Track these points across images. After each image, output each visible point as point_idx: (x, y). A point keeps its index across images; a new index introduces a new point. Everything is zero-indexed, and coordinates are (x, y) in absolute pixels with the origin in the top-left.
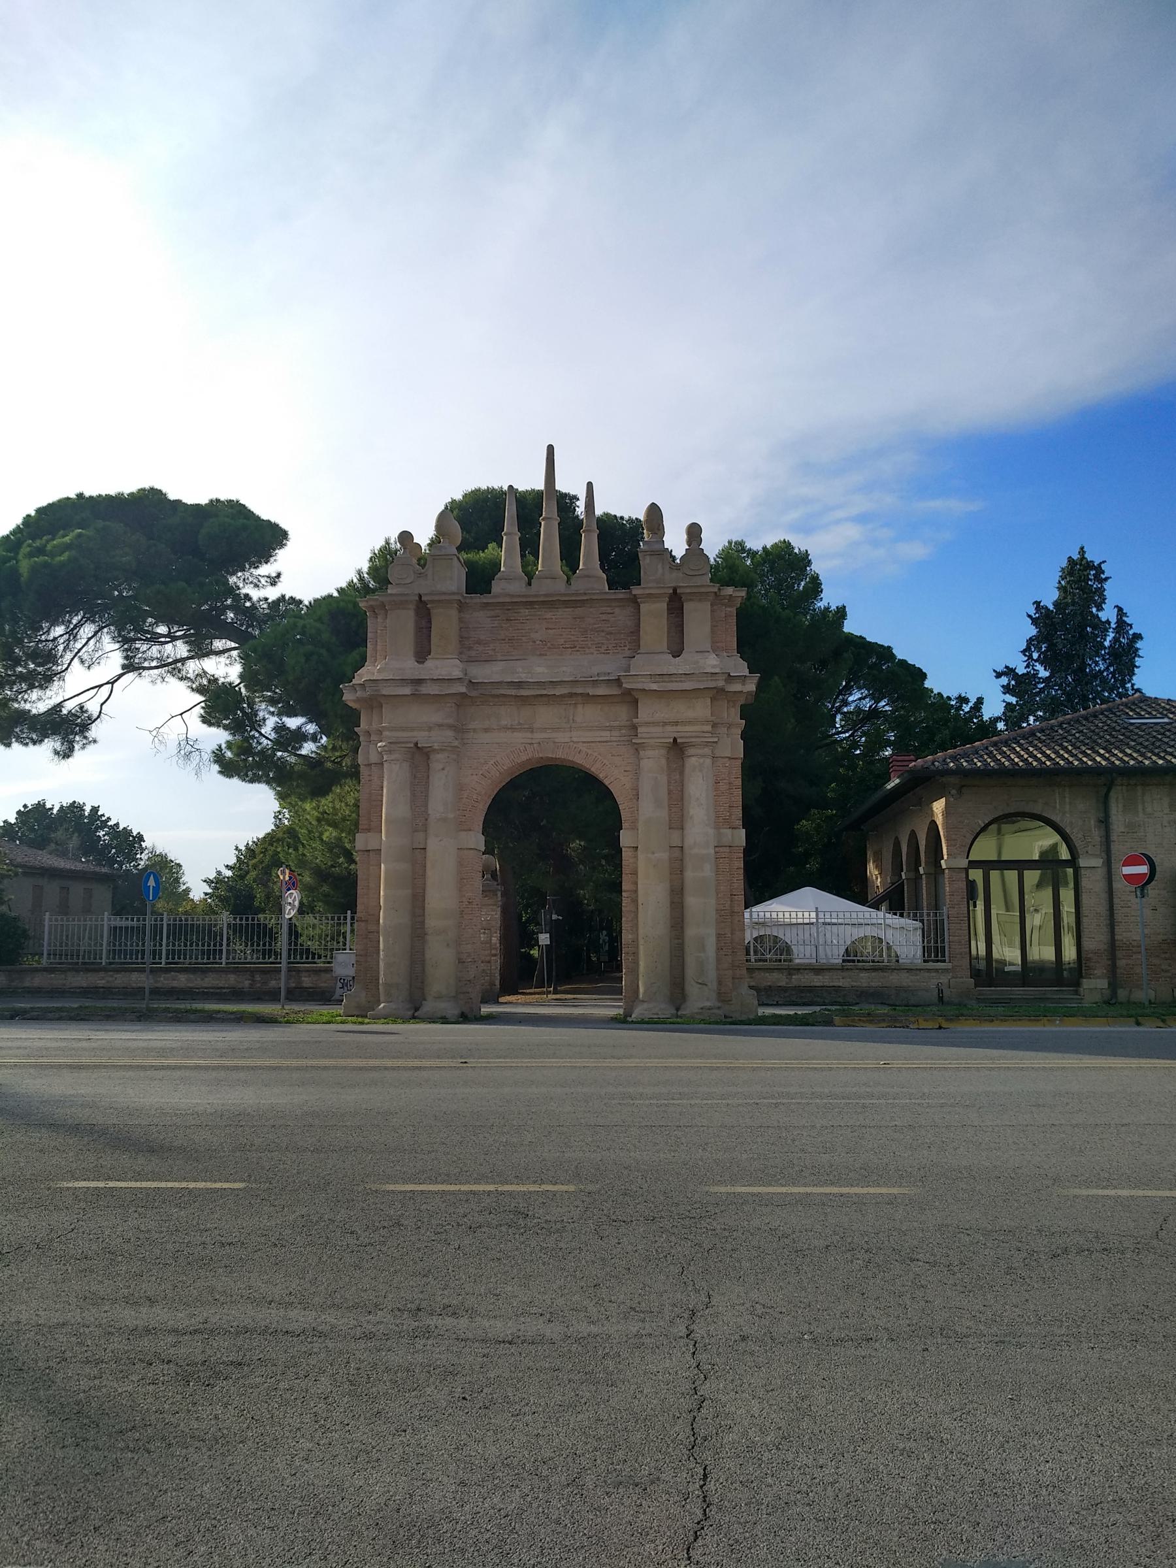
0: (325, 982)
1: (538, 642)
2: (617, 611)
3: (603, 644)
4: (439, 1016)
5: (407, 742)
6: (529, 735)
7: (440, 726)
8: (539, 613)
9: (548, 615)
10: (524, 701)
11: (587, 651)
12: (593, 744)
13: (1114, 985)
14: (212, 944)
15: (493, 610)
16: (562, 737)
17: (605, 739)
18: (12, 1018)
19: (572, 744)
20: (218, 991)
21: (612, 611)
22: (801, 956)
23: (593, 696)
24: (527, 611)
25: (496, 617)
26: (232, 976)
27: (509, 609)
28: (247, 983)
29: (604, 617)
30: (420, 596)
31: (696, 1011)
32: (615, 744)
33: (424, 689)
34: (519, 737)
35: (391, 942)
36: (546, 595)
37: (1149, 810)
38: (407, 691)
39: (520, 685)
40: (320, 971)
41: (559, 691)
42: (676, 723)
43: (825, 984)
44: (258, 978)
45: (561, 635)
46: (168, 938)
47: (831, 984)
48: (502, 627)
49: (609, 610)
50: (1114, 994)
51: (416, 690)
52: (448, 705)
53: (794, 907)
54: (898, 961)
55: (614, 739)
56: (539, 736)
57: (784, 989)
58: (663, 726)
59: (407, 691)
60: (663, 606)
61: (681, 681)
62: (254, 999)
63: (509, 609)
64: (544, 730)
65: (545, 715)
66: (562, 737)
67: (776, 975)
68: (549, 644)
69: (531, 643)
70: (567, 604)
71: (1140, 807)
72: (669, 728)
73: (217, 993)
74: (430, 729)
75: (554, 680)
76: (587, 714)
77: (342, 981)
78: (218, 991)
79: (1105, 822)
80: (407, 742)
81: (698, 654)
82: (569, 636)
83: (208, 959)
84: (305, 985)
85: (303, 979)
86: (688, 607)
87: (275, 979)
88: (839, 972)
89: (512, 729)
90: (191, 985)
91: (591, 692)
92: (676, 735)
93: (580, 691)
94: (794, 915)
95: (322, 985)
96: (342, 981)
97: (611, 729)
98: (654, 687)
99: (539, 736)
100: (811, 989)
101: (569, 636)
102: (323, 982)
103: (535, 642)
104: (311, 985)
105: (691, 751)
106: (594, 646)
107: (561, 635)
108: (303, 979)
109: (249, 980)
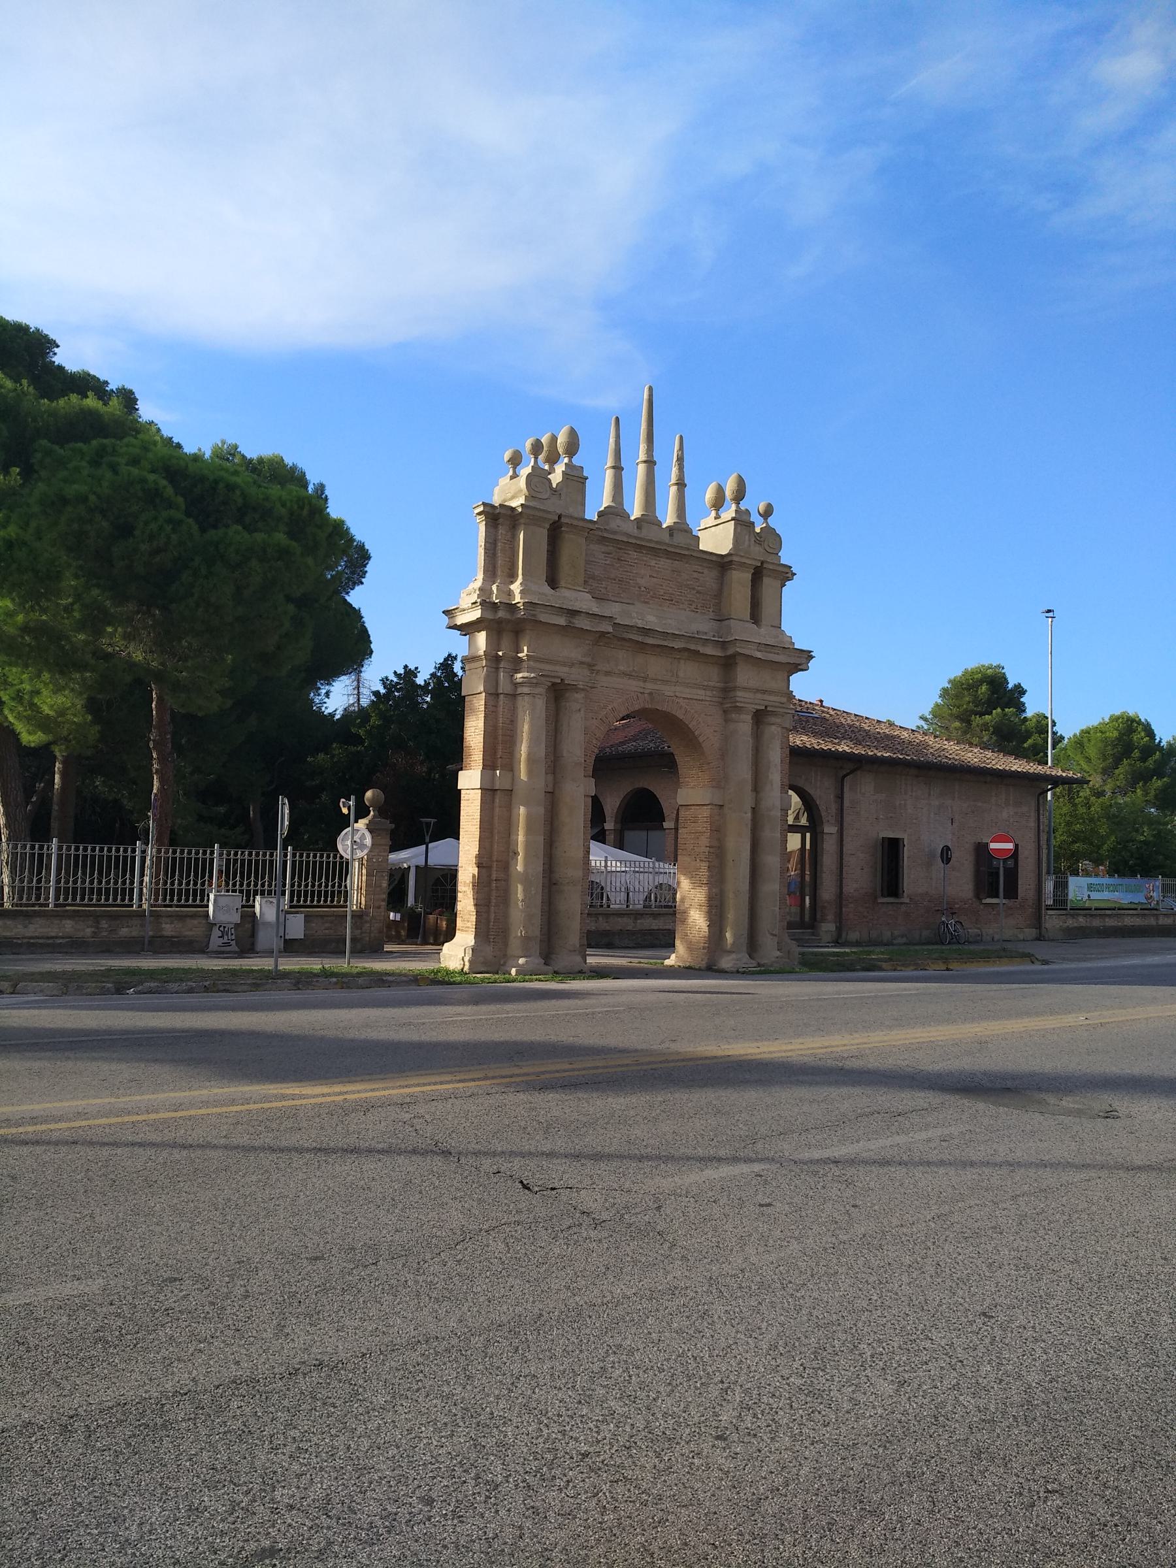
0: (191, 930)
1: (643, 589)
2: (706, 571)
3: (693, 601)
4: (577, 970)
5: (554, 677)
6: (642, 684)
7: (582, 663)
8: (645, 558)
9: (653, 563)
10: (642, 647)
11: (681, 606)
12: (691, 701)
13: (839, 930)
14: (88, 880)
15: (607, 546)
16: (668, 690)
17: (698, 697)
18: (120, 990)
19: (675, 698)
20: (50, 941)
21: (701, 571)
22: (618, 902)
23: (703, 654)
24: (635, 554)
25: (609, 554)
26: (68, 922)
27: (620, 549)
28: (89, 931)
29: (696, 575)
30: (560, 517)
31: (774, 959)
32: (707, 703)
33: (576, 622)
34: (634, 685)
35: (533, 892)
36: (657, 542)
37: (863, 791)
38: (561, 621)
39: (646, 631)
40: (186, 916)
41: (677, 645)
42: (764, 692)
43: (661, 927)
44: (104, 924)
45: (662, 585)
46: (293, 878)
47: (665, 927)
48: (613, 565)
49: (700, 569)
50: (839, 934)
51: (570, 622)
52: (587, 642)
53: (598, 856)
54: (609, 906)
55: (708, 699)
56: (650, 686)
57: (631, 933)
58: (755, 693)
59: (561, 621)
60: (747, 576)
61: (778, 654)
62: (103, 952)
63: (620, 549)
64: (655, 680)
65: (656, 666)
66: (668, 690)
67: (625, 920)
68: (651, 593)
69: (637, 589)
70: (668, 554)
71: (858, 790)
72: (759, 696)
73: (48, 945)
74: (572, 665)
75: (677, 633)
76: (688, 670)
77: (222, 929)
78: (50, 941)
79: (840, 797)
80: (554, 677)
81: (772, 628)
82: (668, 588)
83: (27, 900)
84: (165, 933)
85: (164, 926)
86: (766, 581)
87: (128, 927)
88: (670, 916)
89: (629, 676)
90: (8, 934)
91: (702, 650)
92: (766, 703)
93: (693, 647)
94: (646, 864)
95: (187, 933)
96: (222, 929)
97: (705, 688)
98: (759, 655)
99: (650, 686)
100: (651, 932)
101: (668, 588)
102: (191, 929)
103: (640, 588)
104: (173, 933)
105: (773, 719)
106: (686, 603)
107: (662, 585)
108: (164, 926)
109: (91, 927)
